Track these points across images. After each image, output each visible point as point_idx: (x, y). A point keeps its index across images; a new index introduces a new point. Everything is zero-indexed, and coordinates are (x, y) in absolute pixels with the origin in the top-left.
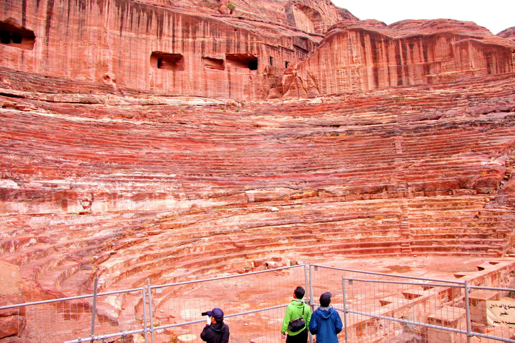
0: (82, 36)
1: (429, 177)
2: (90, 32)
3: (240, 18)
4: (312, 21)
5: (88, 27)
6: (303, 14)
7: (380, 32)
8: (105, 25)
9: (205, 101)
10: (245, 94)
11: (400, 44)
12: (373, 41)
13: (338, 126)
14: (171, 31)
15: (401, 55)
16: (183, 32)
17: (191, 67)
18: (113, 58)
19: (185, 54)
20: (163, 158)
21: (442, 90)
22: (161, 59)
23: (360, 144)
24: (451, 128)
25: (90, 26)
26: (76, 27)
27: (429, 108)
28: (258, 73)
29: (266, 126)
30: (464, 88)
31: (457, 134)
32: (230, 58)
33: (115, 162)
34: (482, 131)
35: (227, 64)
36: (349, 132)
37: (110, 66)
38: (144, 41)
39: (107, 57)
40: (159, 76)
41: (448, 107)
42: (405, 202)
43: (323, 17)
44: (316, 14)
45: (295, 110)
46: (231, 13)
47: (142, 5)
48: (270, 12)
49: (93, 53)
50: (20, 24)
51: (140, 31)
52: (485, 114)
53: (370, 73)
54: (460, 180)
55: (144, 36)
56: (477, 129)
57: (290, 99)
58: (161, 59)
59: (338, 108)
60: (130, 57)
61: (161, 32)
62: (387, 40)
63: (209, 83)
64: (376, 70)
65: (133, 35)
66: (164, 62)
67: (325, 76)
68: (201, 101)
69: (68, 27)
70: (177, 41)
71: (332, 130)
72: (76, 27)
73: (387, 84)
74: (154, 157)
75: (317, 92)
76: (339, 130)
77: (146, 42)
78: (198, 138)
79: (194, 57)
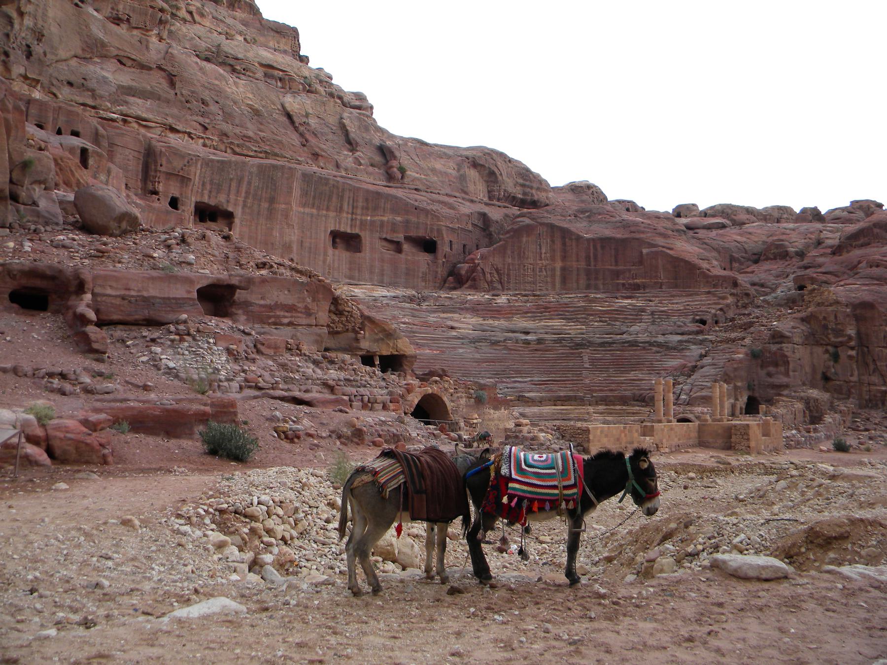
0: (271, 214)
1: (612, 390)
3: (416, 189)
4: (487, 182)
6: (477, 174)
7: (572, 229)
10: (423, 281)
11: (591, 245)
12: (563, 238)
13: (527, 333)
14: (351, 207)
15: (592, 255)
16: (362, 209)
19: (362, 234)
21: (629, 301)
22: (338, 238)
23: (549, 355)
24: (633, 346)
27: (615, 321)
28: (436, 258)
29: (460, 328)
30: (651, 301)
31: (638, 353)
32: (408, 239)
34: (658, 352)
35: (406, 247)
36: (540, 341)
38: (324, 218)
40: (336, 258)
41: (634, 321)
42: (591, 409)
43: (500, 178)
44: (492, 174)
45: (483, 310)
46: (402, 178)
47: (326, 179)
48: (441, 172)
50: (225, 207)
52: (663, 335)
53: (558, 273)
54: (634, 394)
55: (324, 212)
56: (654, 349)
57: (474, 295)
58: (338, 238)
59: (527, 313)
60: (311, 238)
61: (341, 208)
62: (579, 238)
63: (385, 268)
64: (563, 269)
65: (314, 211)
66: (338, 240)
67: (509, 269)
68: (385, 293)
69: (260, 205)
70: (356, 219)
71: (523, 337)
73: (575, 285)
75: (500, 287)
76: (529, 337)
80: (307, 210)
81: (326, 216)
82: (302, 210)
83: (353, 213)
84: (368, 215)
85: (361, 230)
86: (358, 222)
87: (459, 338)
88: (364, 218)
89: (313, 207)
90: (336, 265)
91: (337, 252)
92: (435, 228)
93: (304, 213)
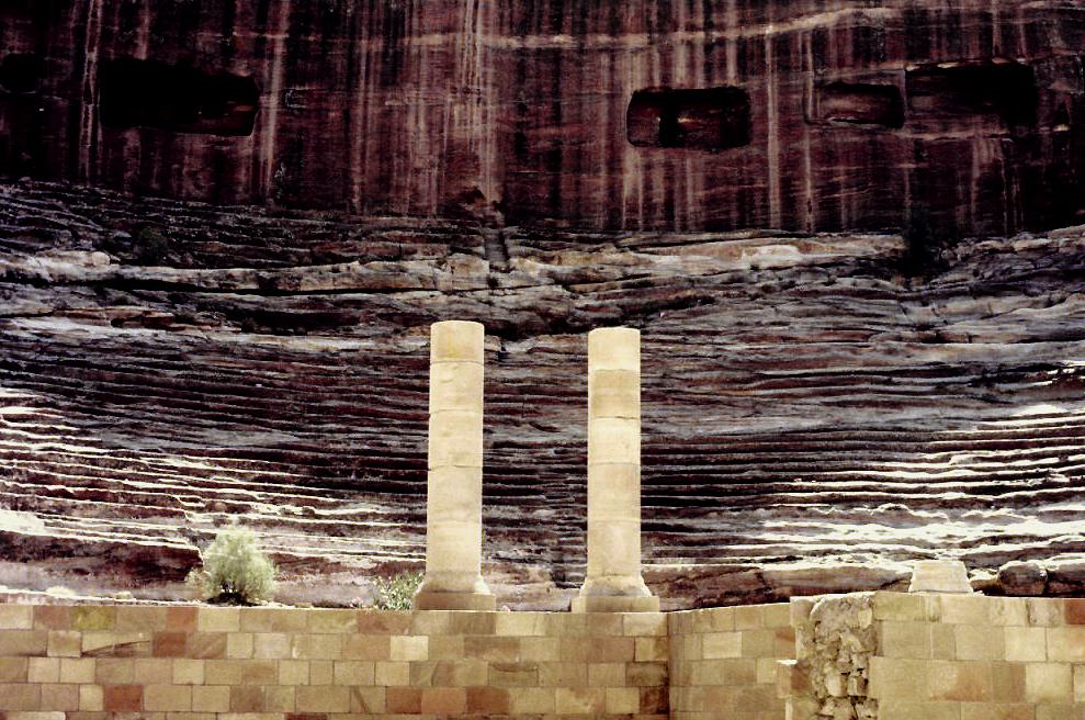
0: (394, 71)
2: (419, 56)
5: (416, 41)
8: (468, 26)
9: (805, 249)
17: (773, 126)
18: (498, 131)
20: (543, 460)
25: (420, 34)
26: (378, 45)
33: (375, 474)
37: (488, 156)
38: (605, 60)
39: (477, 129)
49: (430, 124)
51: (588, 21)
55: (604, 39)
65: (562, 40)
70: (722, 42)
72: (378, 45)
74: (517, 457)
77: (613, 59)
78: (708, 388)
79: (785, 91)
80: (532, 42)
81: (612, 52)
82: (515, 43)
83: (709, 26)
84: (762, 21)
85: (743, 70)
86: (731, 52)
87: (940, 370)
88: (749, 33)
89: (558, 30)
90: (659, 197)
91: (659, 156)
92: (1020, 22)
93: (522, 52)
